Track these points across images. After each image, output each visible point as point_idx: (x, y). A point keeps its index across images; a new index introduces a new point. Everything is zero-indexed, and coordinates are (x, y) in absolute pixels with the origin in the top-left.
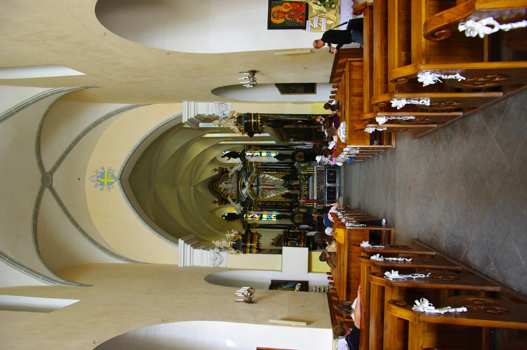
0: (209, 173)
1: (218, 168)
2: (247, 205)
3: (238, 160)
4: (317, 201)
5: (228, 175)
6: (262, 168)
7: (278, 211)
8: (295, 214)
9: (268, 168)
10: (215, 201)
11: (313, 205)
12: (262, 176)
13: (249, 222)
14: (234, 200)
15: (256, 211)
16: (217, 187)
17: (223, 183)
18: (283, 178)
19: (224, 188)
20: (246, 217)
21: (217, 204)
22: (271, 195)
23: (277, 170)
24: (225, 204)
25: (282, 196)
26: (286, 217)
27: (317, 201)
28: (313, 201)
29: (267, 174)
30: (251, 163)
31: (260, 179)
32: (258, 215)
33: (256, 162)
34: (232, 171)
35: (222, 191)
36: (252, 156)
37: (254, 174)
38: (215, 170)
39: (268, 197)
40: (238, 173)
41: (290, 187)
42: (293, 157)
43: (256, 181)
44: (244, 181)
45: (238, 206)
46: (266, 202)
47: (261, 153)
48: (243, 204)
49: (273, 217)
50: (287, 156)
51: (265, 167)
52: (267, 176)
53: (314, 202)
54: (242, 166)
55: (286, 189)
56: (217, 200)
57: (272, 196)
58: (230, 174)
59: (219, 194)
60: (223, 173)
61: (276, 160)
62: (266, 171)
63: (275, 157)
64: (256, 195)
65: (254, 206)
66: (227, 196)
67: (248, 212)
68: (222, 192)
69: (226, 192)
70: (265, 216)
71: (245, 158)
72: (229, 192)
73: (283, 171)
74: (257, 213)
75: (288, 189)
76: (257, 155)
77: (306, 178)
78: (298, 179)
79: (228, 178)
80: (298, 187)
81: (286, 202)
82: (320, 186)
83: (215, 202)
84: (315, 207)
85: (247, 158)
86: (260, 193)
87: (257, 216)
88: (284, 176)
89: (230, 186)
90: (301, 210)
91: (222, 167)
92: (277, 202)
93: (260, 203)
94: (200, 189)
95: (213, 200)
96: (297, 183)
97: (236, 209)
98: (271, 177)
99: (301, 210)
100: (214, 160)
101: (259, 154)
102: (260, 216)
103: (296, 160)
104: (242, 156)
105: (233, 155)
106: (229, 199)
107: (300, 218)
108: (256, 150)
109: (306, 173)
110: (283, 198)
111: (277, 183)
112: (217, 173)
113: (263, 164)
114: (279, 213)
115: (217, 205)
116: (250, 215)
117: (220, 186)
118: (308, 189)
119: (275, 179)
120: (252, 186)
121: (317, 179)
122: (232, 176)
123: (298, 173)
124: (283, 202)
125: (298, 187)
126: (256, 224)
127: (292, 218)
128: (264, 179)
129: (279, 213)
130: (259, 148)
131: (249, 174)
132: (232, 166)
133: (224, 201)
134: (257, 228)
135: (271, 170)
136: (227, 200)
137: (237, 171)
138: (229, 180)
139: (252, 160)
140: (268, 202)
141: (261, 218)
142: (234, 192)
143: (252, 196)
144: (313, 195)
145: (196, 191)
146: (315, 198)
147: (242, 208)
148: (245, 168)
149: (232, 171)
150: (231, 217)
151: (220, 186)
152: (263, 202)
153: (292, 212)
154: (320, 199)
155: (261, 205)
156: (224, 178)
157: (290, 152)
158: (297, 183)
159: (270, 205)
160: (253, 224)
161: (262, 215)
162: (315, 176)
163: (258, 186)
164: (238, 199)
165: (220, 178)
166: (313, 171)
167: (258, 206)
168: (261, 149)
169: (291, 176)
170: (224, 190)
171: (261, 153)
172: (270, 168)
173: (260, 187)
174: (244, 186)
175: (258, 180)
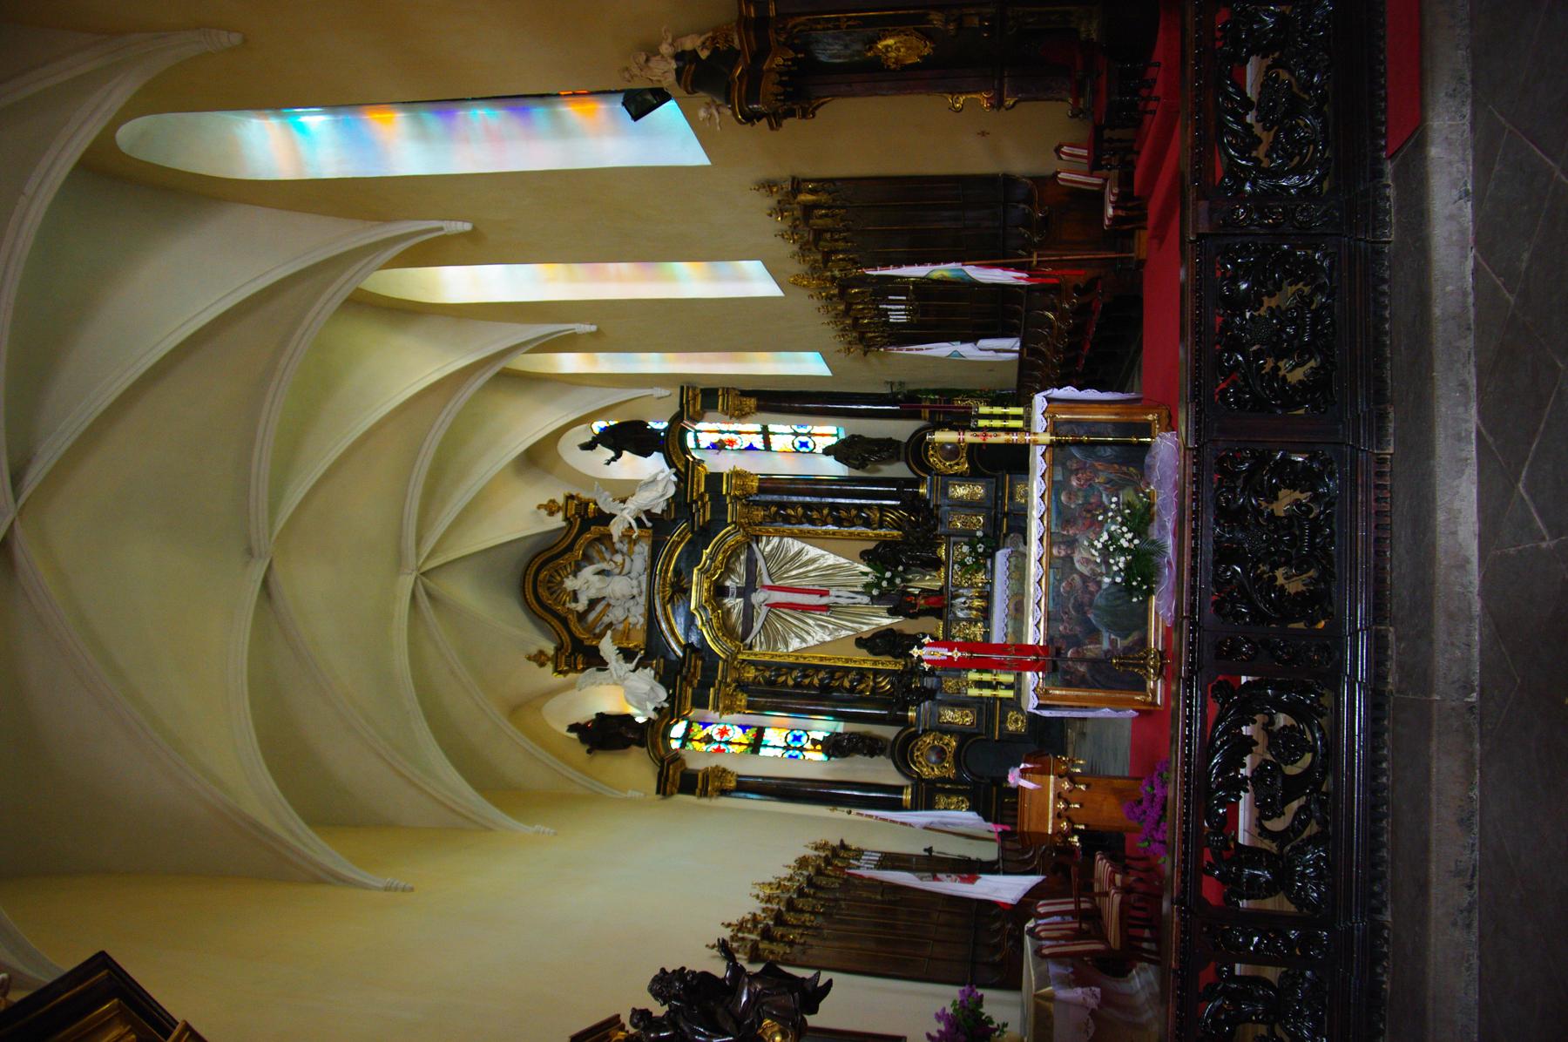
0: (523, 515)
1: (561, 501)
2: (690, 679)
3: (654, 465)
4: (1049, 659)
5: (610, 536)
6: (766, 505)
7: (839, 716)
8: (915, 736)
9: (793, 505)
10: (541, 652)
11: (1016, 686)
12: (768, 545)
13: (693, 765)
14: (627, 654)
15: (730, 709)
16: (555, 587)
17: (588, 572)
18: (866, 556)
19: (593, 594)
20: (686, 738)
21: (550, 667)
22: (811, 639)
23: (839, 517)
24: (587, 666)
25: (861, 642)
26: (870, 747)
27: (1049, 659)
28: (1019, 656)
29: (793, 536)
30: (714, 479)
31: (761, 563)
32: (744, 728)
33: (738, 474)
34: (624, 517)
35: (581, 606)
36: (717, 447)
37: (729, 536)
38: (551, 508)
39: (795, 644)
40: (656, 525)
41: (901, 604)
42: (916, 450)
43: (741, 569)
44: (682, 565)
45: (644, 681)
46: (779, 668)
47: (765, 433)
48: (667, 677)
49: (809, 746)
50: (887, 449)
51: (786, 503)
52: (795, 545)
53: (1023, 667)
54: (672, 491)
55: (882, 609)
56: (549, 648)
57: (811, 642)
58: (616, 529)
59: (564, 621)
60: (586, 524)
61: (833, 468)
62: (787, 520)
63: (827, 451)
64: (738, 634)
65: (724, 682)
66: (601, 636)
67: (695, 713)
68: (581, 616)
69: (603, 613)
70: (774, 736)
71: (686, 451)
72: (616, 615)
73: (867, 523)
74: (736, 717)
75: (892, 613)
76: (751, 448)
77: (977, 556)
78: (936, 564)
79: (616, 552)
80: (938, 605)
81: (876, 673)
82: (1071, 543)
83: (539, 659)
84: (1031, 703)
85: (697, 455)
86: (757, 626)
87: (736, 734)
88: (871, 545)
89: (619, 587)
90: (949, 715)
91: (585, 495)
92: (833, 670)
93: (751, 673)
94: (464, 592)
95: (534, 650)
96: (932, 581)
97: (631, 696)
98: (812, 551)
99: (949, 715)
100: (538, 458)
101: (758, 442)
102: (751, 733)
103: (928, 469)
104: (670, 444)
105: (629, 437)
106: (607, 648)
107: (941, 753)
108: (741, 415)
109: (969, 437)
110: (863, 654)
111: (838, 580)
112: (558, 521)
113: (770, 485)
114: (840, 727)
115: (547, 676)
116: (705, 725)
117: (570, 583)
118: (986, 614)
119: (831, 559)
120: (720, 591)
121: (1055, 488)
122: (627, 535)
123: (940, 529)
124: (862, 673)
125: (938, 605)
126: (722, 773)
127: (901, 754)
128: (782, 561)
129: (840, 727)
130: (752, 402)
131: (704, 535)
132: (625, 490)
133: (579, 655)
134: (724, 792)
135: (809, 514)
136: (596, 649)
137: (648, 513)
138: (618, 558)
139: (721, 463)
140: (791, 667)
141: (756, 745)
142: (638, 618)
143: (716, 639)
144: (1018, 610)
145: (426, 596)
146: (1034, 635)
147: (662, 694)
148: (681, 503)
149: (624, 517)
150: (607, 734)
151: (570, 583)
152: (767, 666)
153: (903, 721)
154: (1075, 642)
155: (755, 681)
156: (591, 543)
157: (901, 430)
158: (932, 581)
159: (797, 685)
160: (707, 775)
161: (760, 731)
162: (1038, 463)
163: (744, 593)
164: (648, 651)
165: (570, 548)
166: (1027, 429)
167: (742, 686)
168: (761, 408)
169: (907, 546)
170: (593, 603)
171: (765, 433)
172: (807, 506)
173: (758, 597)
174: (680, 590)
175: (751, 563)
